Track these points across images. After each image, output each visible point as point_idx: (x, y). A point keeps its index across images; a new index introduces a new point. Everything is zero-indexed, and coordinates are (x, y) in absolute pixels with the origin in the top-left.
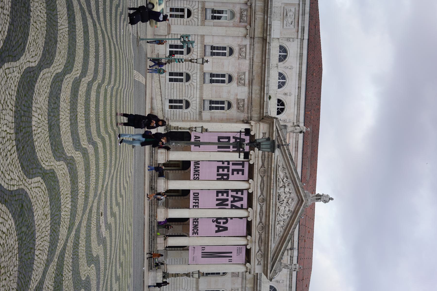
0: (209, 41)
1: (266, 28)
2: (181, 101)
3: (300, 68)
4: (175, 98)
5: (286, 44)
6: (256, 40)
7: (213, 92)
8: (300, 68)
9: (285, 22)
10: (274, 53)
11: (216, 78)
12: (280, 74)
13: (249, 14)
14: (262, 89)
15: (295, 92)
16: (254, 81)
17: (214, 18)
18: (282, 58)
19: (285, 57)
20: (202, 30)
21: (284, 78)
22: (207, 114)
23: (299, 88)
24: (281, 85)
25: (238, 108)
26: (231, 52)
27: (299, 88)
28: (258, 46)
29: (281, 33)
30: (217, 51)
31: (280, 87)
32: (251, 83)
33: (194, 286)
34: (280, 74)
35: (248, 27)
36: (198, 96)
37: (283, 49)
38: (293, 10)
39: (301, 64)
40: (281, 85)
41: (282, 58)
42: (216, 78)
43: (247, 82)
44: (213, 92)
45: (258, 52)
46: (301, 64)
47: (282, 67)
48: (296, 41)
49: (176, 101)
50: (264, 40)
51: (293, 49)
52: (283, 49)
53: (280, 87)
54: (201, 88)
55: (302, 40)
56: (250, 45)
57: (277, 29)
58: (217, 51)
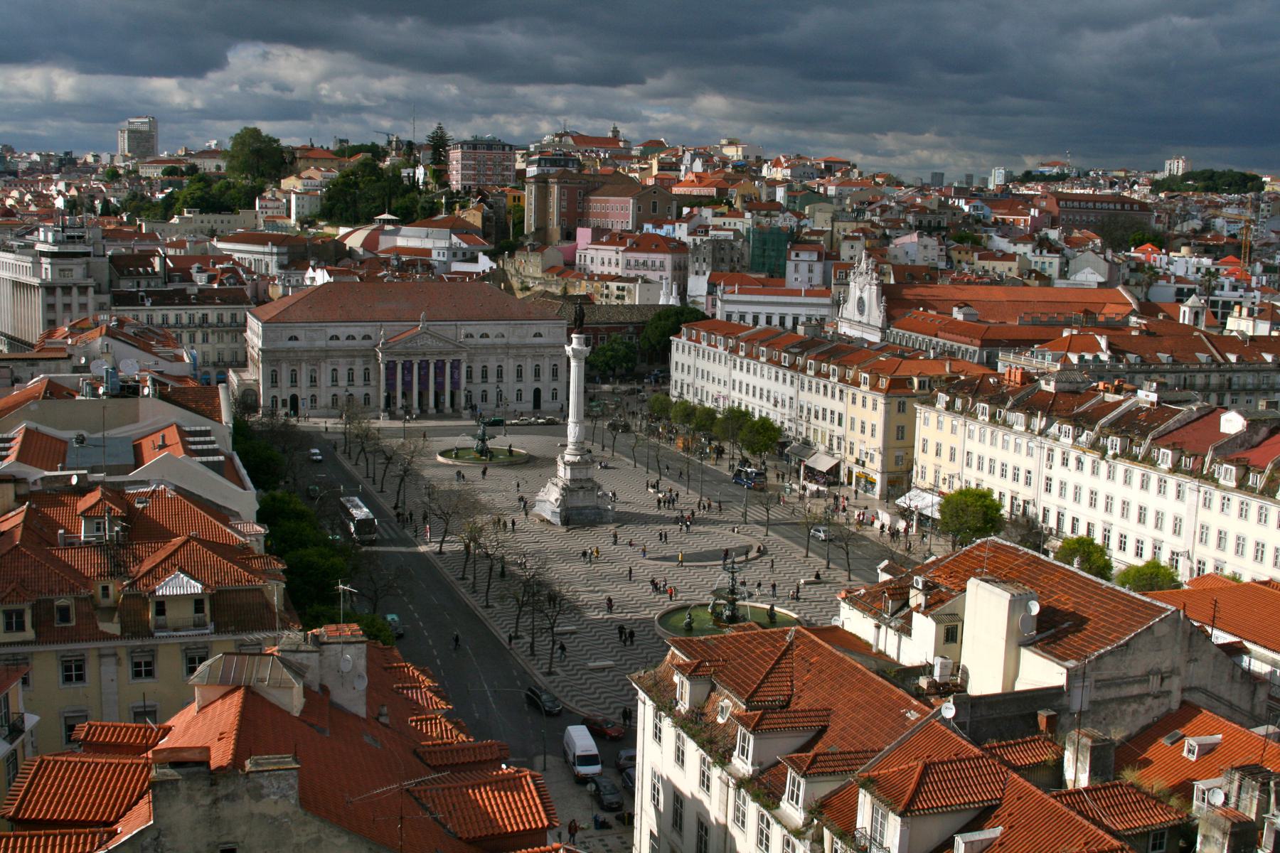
0: (329, 384)
1: (322, 350)
7: (359, 380)
11: (351, 379)
18: (337, 338)
20: (323, 387)
22: (373, 383)
24: (354, 338)
26: (334, 370)
30: (335, 380)
32: (354, 356)
37: (332, 338)
40: (354, 338)
41: (337, 338)
42: (351, 379)
44: (359, 380)
52: (332, 338)
57: (321, 343)
58: (335, 380)
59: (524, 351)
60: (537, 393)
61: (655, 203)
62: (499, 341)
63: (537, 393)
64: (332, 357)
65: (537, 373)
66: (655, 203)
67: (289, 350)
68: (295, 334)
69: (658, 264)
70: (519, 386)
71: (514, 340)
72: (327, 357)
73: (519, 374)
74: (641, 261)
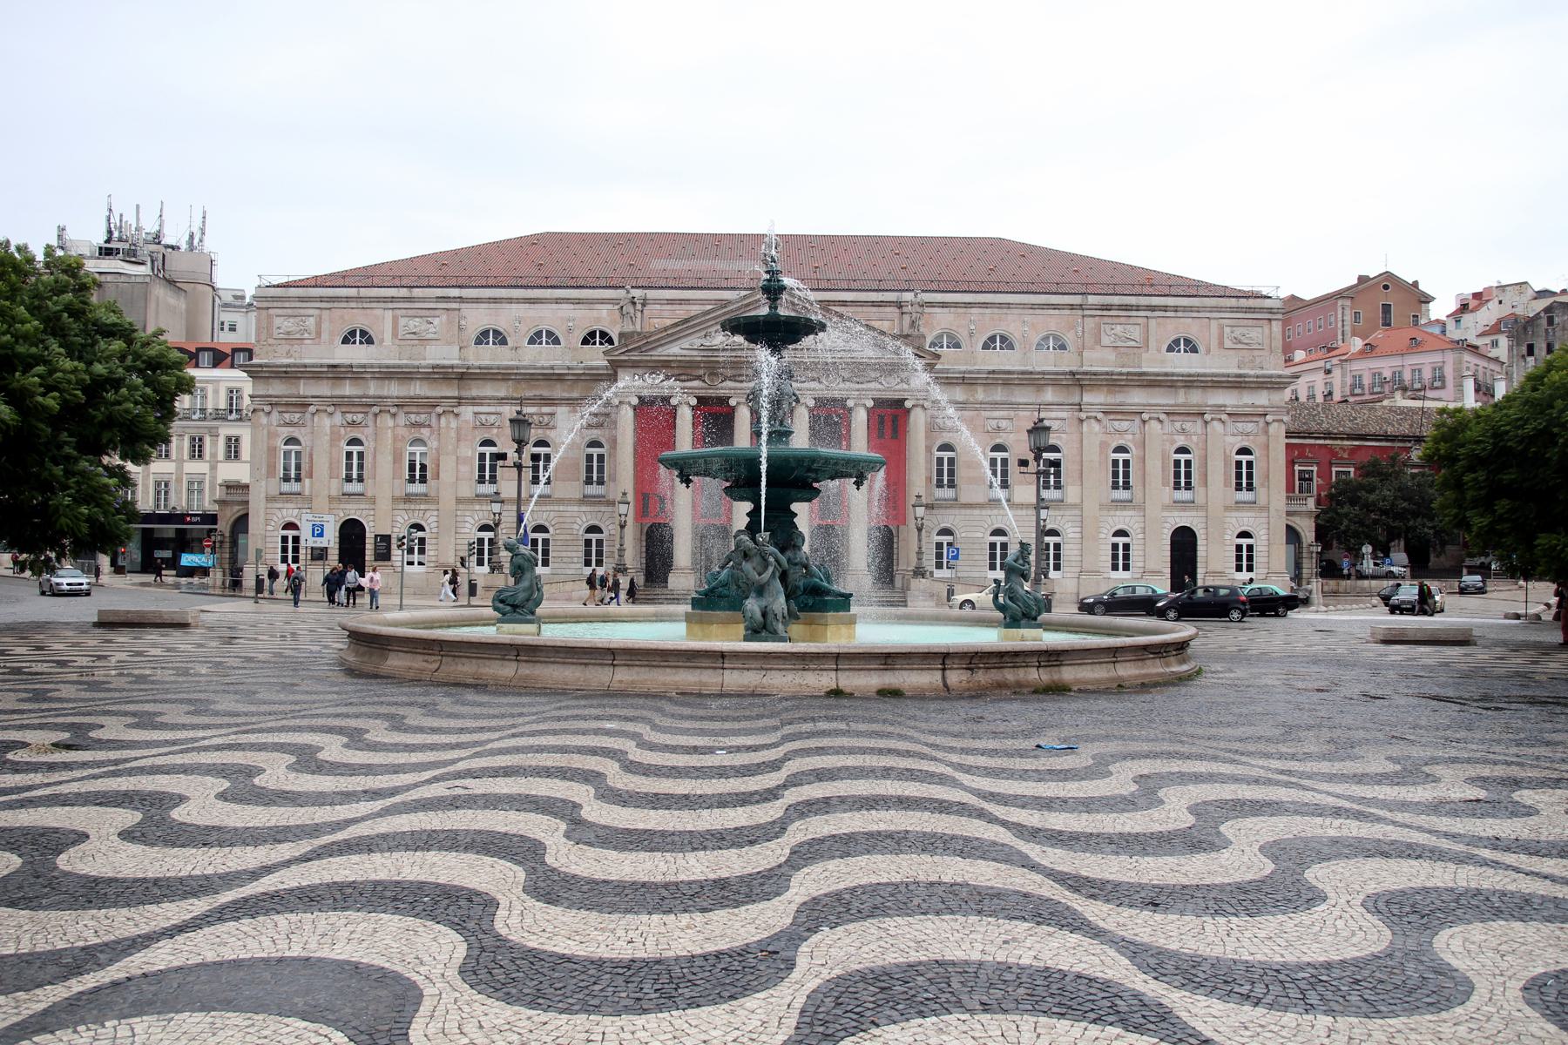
1: (442, 374)
2: (588, 543)
3: (519, 301)
4: (582, 554)
5: (473, 332)
6: (464, 394)
8: (519, 301)
9: (431, 336)
10: (489, 356)
12: (532, 341)
13: (414, 409)
14: (560, 378)
15: (566, 310)
16: (546, 393)
17: (423, 480)
19: (497, 333)
21: (539, 334)
23: (558, 301)
25: (600, 426)
27: (558, 301)
28: (475, 390)
29: (449, 344)
31: (557, 341)
33: (977, 512)
34: (532, 341)
35: (439, 410)
36: (576, 508)
38: (402, 321)
39: (510, 300)
43: (546, 409)
45: (489, 390)
46: (510, 300)
47: (518, 338)
48: (464, 312)
49: (588, 553)
50: (463, 376)
51: (478, 318)
53: (557, 341)
54: (561, 501)
55: (461, 299)
56: (474, 404)
59: (1137, 397)
60: (1184, 545)
61: (1386, 309)
62: (1046, 361)
63: (1184, 545)
64: (474, 401)
65: (1182, 477)
66: (1386, 309)
67: (336, 373)
68: (359, 320)
69: (1427, 375)
70: (1123, 519)
71: (1100, 360)
72: (460, 401)
73: (1121, 476)
74: (1387, 374)
